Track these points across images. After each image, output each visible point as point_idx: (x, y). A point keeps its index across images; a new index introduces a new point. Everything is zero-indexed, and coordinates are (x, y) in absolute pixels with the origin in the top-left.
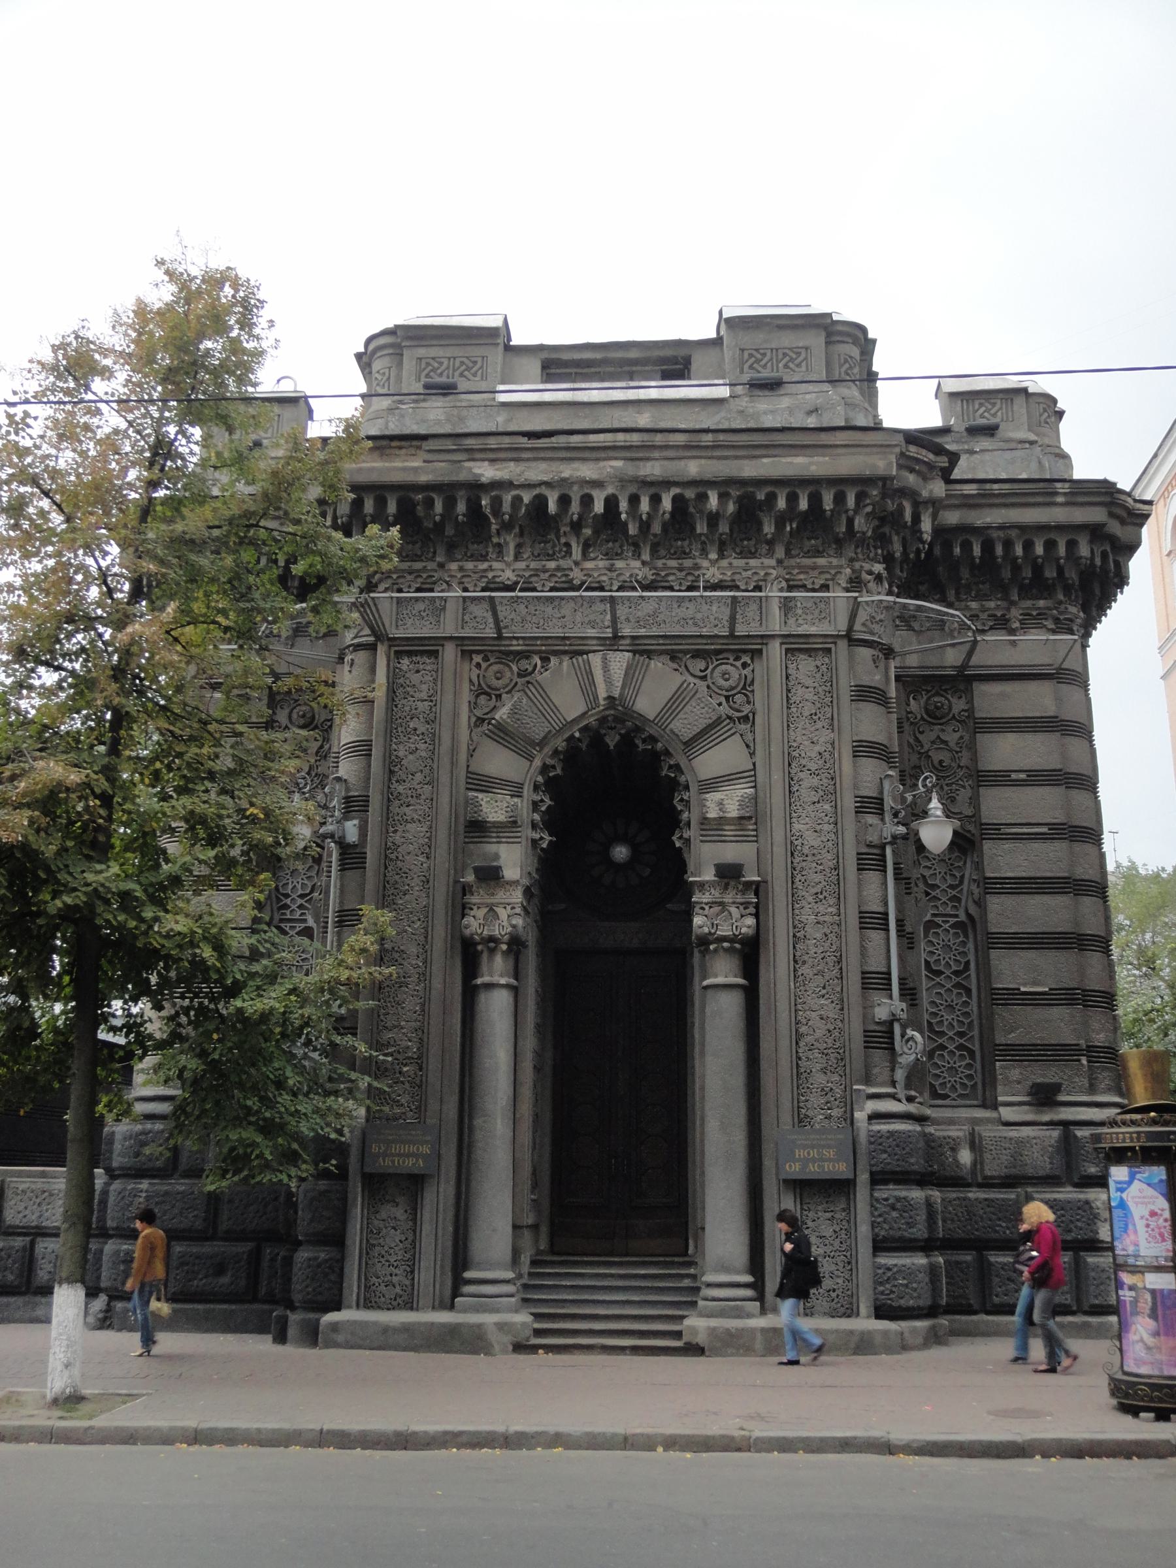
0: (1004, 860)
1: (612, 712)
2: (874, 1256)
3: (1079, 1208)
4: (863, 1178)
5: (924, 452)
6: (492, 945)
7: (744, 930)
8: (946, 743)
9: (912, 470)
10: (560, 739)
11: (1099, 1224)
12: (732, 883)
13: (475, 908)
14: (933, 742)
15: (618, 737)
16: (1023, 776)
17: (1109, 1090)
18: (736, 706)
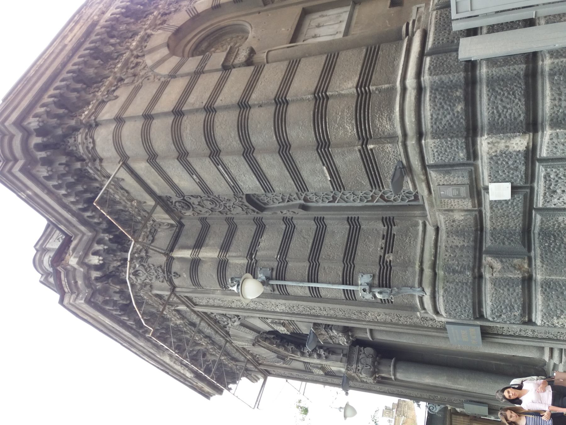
0: (249, 183)
2: (534, 324)
3: (497, 163)
4: (478, 323)
5: (63, 283)
8: (199, 202)
9: (76, 282)
11: (511, 149)
14: (203, 207)
16: (195, 177)
17: (390, 119)
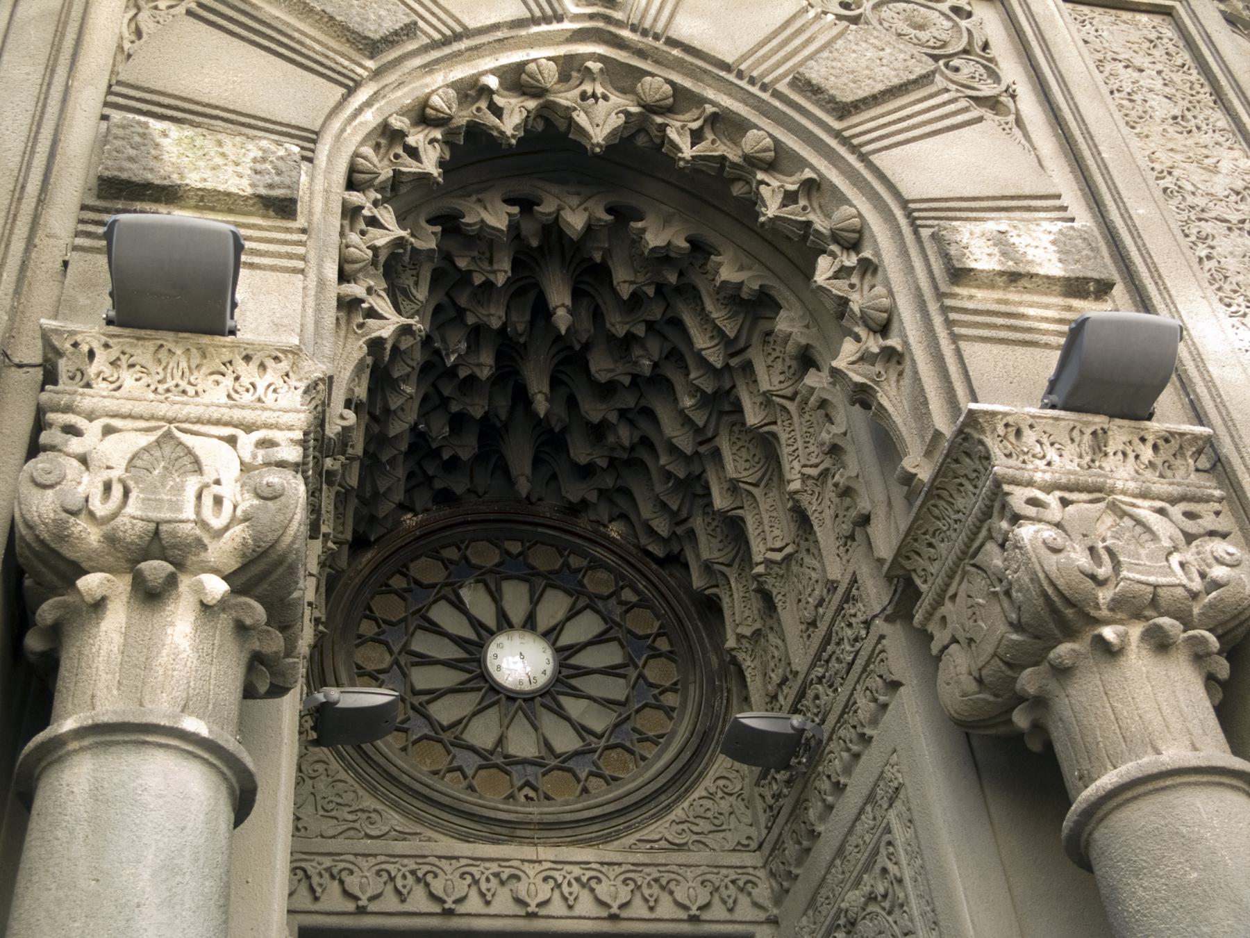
1: (601, 49)
6: (155, 568)
7: (1218, 572)
10: (439, 79)
12: (1119, 433)
13: (93, 429)
15: (617, 121)
18: (961, 77)
